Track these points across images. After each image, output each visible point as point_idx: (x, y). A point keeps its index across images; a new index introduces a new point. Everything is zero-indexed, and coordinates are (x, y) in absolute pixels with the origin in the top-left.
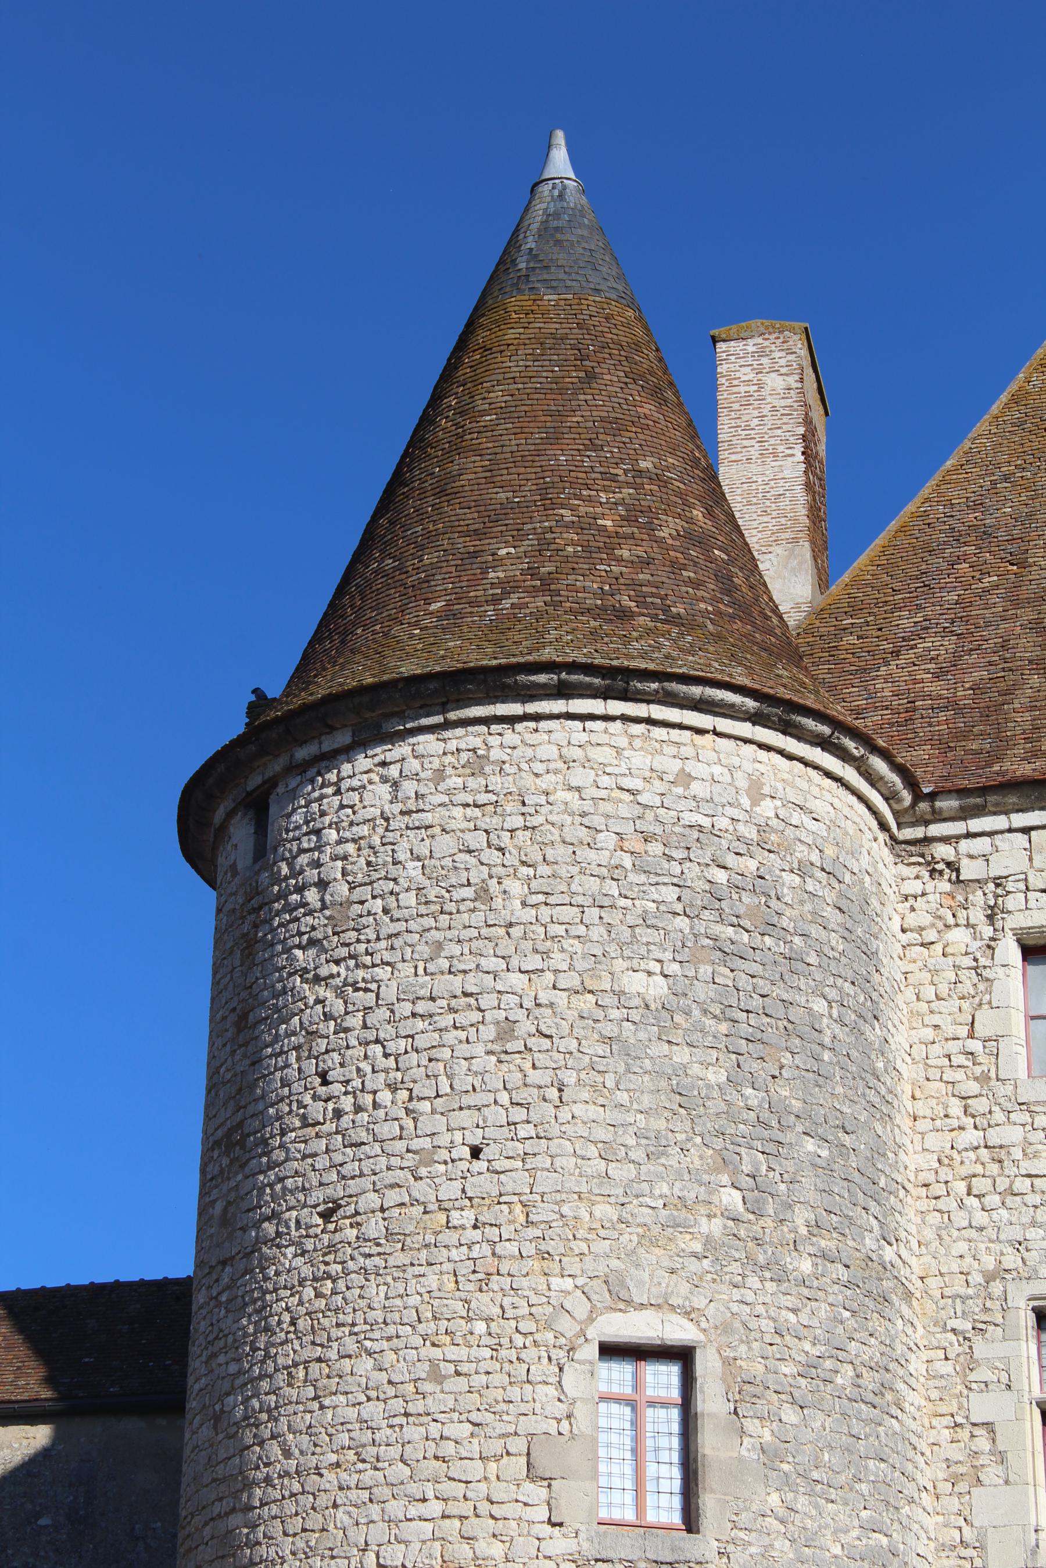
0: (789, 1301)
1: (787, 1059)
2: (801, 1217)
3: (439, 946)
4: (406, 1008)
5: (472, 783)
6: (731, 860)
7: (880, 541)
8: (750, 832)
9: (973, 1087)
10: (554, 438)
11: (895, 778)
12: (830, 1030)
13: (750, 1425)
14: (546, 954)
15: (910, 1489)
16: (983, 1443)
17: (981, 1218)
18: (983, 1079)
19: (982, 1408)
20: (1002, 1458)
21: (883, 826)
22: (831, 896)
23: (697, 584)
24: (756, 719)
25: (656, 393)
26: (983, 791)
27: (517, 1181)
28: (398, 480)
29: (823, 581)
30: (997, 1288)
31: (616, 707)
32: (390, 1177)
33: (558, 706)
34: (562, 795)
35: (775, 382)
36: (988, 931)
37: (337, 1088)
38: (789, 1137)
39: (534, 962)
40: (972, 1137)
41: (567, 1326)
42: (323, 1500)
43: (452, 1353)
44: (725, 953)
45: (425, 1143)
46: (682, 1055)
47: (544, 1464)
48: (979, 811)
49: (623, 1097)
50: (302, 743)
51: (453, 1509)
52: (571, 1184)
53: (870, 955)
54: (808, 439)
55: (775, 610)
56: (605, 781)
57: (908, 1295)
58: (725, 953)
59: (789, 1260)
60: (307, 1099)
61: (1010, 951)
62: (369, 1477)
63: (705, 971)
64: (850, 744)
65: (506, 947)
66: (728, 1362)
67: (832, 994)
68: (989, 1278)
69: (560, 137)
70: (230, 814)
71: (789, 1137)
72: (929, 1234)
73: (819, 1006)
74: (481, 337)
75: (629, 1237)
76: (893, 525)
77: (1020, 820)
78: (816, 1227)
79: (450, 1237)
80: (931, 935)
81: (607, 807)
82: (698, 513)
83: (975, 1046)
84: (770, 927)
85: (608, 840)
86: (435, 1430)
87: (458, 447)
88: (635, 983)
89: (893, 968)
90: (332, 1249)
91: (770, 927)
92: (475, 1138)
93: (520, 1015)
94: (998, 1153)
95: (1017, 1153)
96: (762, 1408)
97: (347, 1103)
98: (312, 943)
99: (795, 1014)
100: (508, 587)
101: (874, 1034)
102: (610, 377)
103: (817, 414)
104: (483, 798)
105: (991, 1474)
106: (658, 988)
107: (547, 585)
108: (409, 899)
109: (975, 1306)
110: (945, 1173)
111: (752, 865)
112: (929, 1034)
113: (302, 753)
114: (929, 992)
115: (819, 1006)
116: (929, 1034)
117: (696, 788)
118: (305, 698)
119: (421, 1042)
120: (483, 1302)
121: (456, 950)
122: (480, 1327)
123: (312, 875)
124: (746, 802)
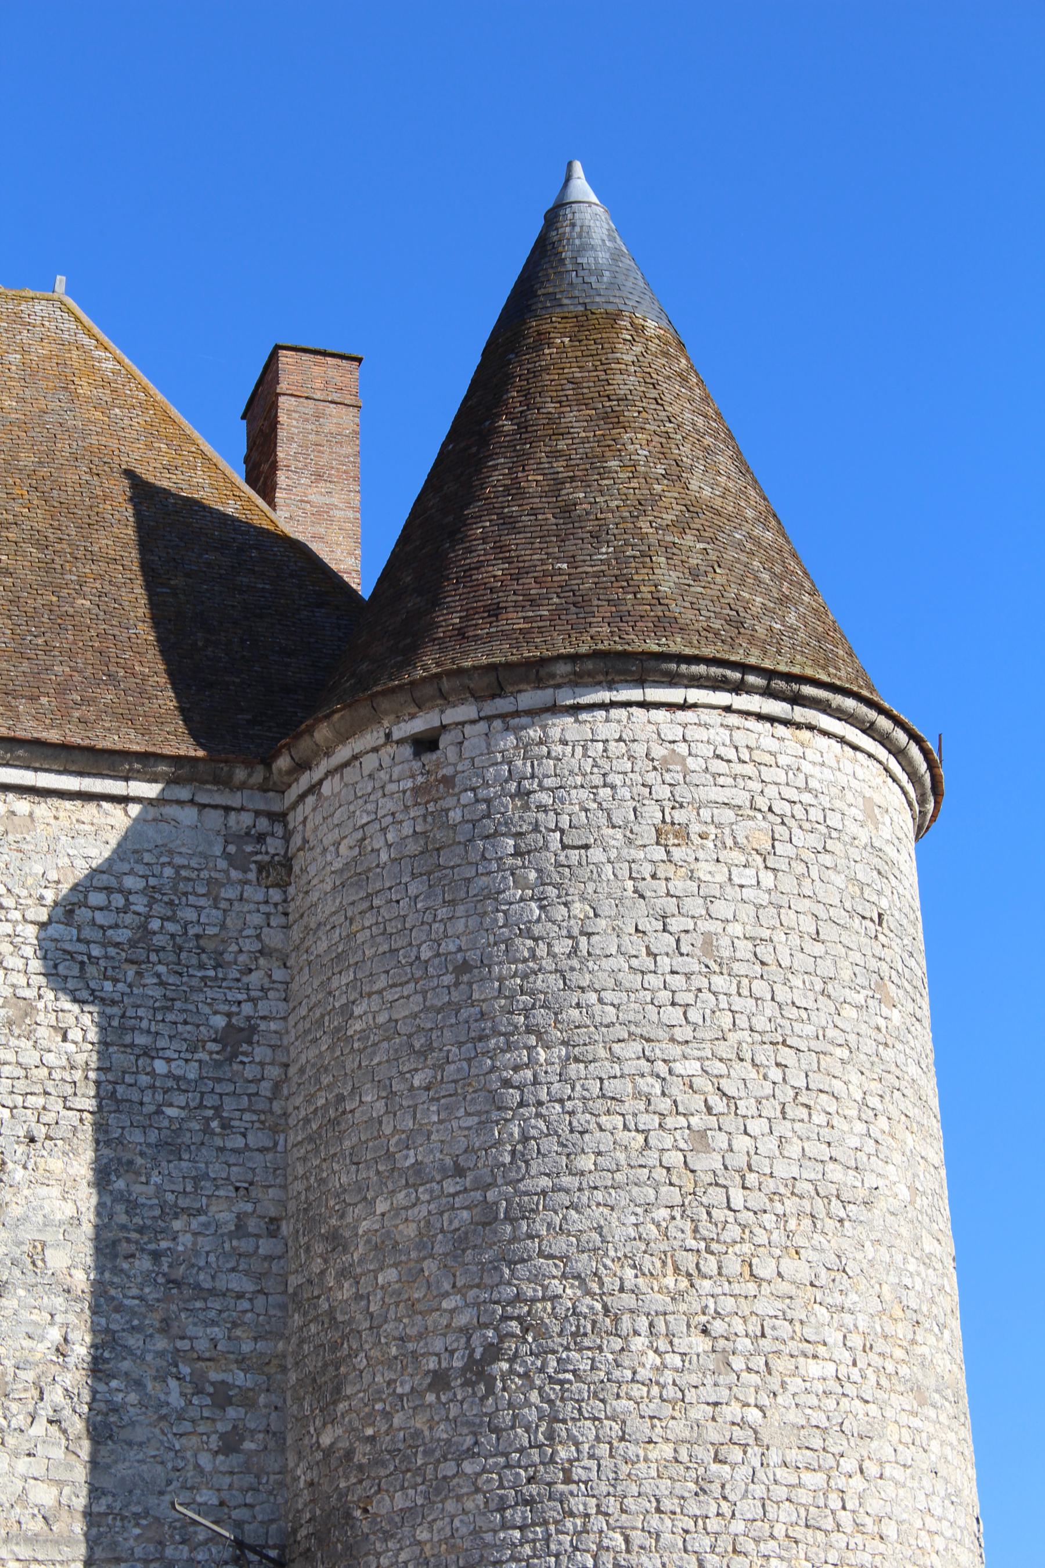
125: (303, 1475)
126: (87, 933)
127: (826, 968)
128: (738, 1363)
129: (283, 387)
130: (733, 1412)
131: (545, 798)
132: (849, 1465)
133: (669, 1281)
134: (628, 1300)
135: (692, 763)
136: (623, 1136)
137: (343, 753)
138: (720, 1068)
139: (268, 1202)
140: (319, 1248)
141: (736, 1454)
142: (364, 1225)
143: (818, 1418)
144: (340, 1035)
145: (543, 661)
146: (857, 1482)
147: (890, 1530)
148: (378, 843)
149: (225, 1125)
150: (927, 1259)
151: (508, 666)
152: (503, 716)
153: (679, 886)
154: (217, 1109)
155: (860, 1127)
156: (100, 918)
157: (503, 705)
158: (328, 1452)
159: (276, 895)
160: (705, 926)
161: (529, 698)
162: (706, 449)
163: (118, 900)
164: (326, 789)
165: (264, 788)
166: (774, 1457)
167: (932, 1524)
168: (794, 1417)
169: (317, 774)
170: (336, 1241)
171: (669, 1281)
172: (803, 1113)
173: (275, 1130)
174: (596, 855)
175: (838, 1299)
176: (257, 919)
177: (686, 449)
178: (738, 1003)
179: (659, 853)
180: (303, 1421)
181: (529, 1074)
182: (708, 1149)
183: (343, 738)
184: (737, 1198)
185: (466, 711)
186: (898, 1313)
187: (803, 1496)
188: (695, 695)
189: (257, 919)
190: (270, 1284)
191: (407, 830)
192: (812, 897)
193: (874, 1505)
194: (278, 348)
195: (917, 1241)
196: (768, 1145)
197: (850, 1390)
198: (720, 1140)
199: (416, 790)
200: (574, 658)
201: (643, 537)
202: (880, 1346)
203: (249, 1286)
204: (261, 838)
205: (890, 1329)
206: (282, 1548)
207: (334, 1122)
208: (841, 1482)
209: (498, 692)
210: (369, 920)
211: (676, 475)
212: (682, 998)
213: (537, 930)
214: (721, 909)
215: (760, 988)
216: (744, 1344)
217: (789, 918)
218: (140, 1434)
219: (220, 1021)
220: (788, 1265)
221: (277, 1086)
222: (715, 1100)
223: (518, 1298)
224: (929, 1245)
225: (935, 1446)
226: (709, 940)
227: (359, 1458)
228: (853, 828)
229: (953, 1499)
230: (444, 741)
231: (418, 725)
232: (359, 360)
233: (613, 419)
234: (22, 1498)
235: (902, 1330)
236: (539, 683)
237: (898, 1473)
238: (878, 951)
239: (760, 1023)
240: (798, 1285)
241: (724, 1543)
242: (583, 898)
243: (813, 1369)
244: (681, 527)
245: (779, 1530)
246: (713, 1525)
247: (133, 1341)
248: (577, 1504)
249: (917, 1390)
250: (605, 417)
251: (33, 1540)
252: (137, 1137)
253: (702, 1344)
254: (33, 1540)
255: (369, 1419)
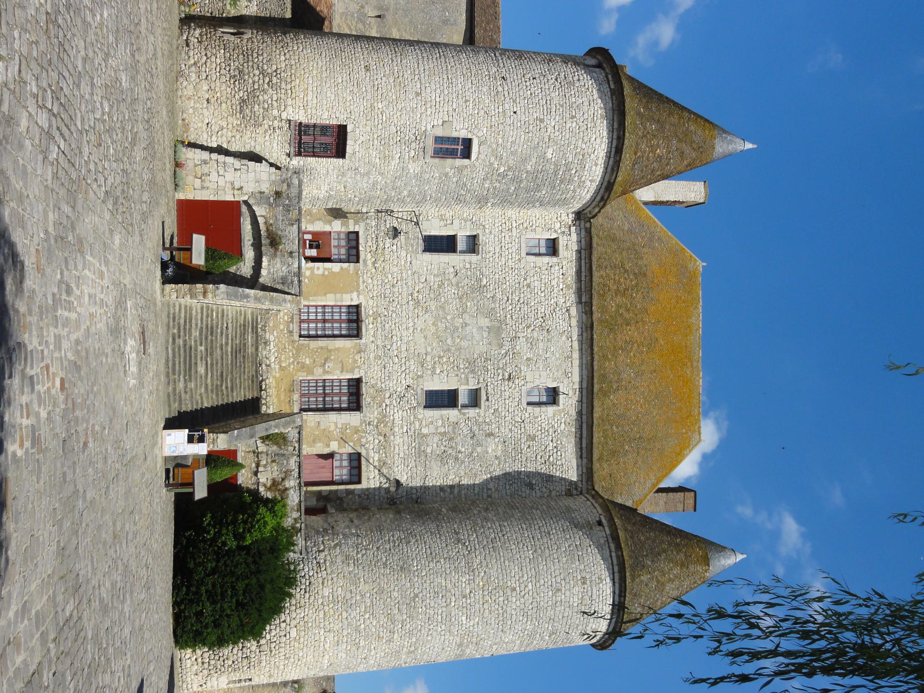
0: (479, 181)
1: (532, 184)
2: (498, 185)
3: (562, 106)
4: (548, 98)
5: (599, 116)
6: (577, 174)
7: (652, 216)
8: (583, 179)
9: (525, 226)
10: (680, 141)
11: (594, 213)
12: (539, 194)
13: (453, 171)
14: (558, 131)
15: (439, 206)
16: (449, 222)
17: (497, 225)
18: (527, 228)
19: (456, 222)
20: (446, 226)
21: (584, 210)
22: (568, 197)
23: (642, 171)
24: (609, 182)
25: (689, 165)
26: (591, 233)
27: (508, 121)
28: (675, 103)
29: (646, 203)
30: (481, 227)
31: (613, 150)
32: (511, 93)
33: (615, 137)
34: (594, 136)
35: (693, 195)
36: (559, 231)
37: (532, 81)
38: (515, 183)
39: (557, 128)
40: (514, 225)
41: (476, 131)
42: (441, 75)
43: (471, 105)
44: (556, 173)
45: (518, 101)
46: (534, 160)
47: (445, 125)
48: (586, 231)
49: (525, 146)
50: (612, 77)
51: (438, 103)
52: (507, 134)
53: (555, 205)
54: (679, 202)
55: (635, 190)
56: (597, 147)
57: (480, 208)
58: (556, 173)
59: (488, 182)
60: (530, 75)
61: (554, 236)
62: (445, 85)
63: (552, 167)
64: (602, 204)
65: (561, 121)
66: (466, 167)
67: (546, 195)
68: (484, 226)
69: (756, 146)
70: (598, 60)
71: (515, 183)
72: (494, 214)
73: (544, 192)
74: (707, 125)
75: (494, 146)
76: (656, 220)
77: (583, 240)
78: (495, 188)
79: (497, 106)
80: (559, 219)
81: (591, 146)
82: (658, 173)
83: (534, 227)
84: (562, 182)
85: (584, 146)
86: (455, 100)
87: (681, 117)
88: (550, 151)
89: (552, 210)
90: (495, 78)
91: (562, 182)
92: (518, 112)
93: (545, 124)
94: (510, 230)
95: (510, 234)
96: (456, 173)
97: (528, 84)
98: (565, 78)
99: (542, 186)
100: (645, 128)
101: (537, 204)
102: (694, 155)
103: (685, 205)
104: (595, 118)
105: (442, 223)
106: (549, 155)
107: (644, 136)
108: (574, 100)
109: (478, 222)
110: (507, 218)
111: (576, 179)
112: (537, 217)
113: (610, 76)
114: (546, 218)
115: (544, 192)
116: (537, 217)
117: (594, 167)
118: (623, 78)
119: (541, 101)
120: (482, 112)
121: (561, 110)
122: (476, 112)
123: (581, 78)
124: (590, 178)
125: (436, 505)
126: (551, 452)
127: (556, 619)
128: (464, 600)
129: (687, 493)
130: (453, 600)
131: (589, 550)
132: (443, 627)
133: (481, 583)
134: (477, 574)
135: (601, 585)
136: (513, 571)
137: (596, 505)
138: (531, 594)
139: (495, 495)
140: (485, 506)
141: (444, 600)
142: (490, 515)
143: (453, 619)
144: (532, 508)
145: (621, 548)
146: (440, 629)
147: (429, 638)
148: (576, 514)
149: (511, 485)
150: (491, 647)
151: (619, 540)
152: (607, 540)
153: (572, 582)
154: (514, 483)
155: (520, 628)
156: (555, 454)
157: (610, 540)
158: (441, 510)
159: (563, 493)
160: (563, 589)
161: (612, 546)
162: (678, 588)
163: (559, 458)
164: (588, 502)
165: (587, 489)
166: (444, 609)
167: (432, 648)
168: (453, 614)
169: (592, 500)
170: (487, 510)
171: (481, 583)
172: (522, 614)
173: (511, 496)
174: (577, 563)
175: (480, 624)
176: (558, 489)
177: (677, 583)
178: (546, 597)
179: (579, 578)
180: (447, 505)
181: (526, 549)
182: (512, 592)
183: (600, 505)
184: (500, 599)
185: (608, 532)
186: (479, 639)
187: (436, 616)
188: (617, 585)
189: (558, 489)
190: (477, 496)
191: (580, 520)
192: (572, 616)
193: (434, 634)
194: (695, 492)
195: (495, 644)
196: (514, 607)
197: (460, 627)
198: (514, 594)
199: (589, 522)
200: (623, 555)
201: (654, 572)
202: (471, 634)
203: (476, 492)
204: (576, 489)
205: (475, 637)
206: (420, 503)
207: (513, 507)
208: (439, 625)
209: (613, 539)
210: (559, 513)
211: (670, 580)
212: (546, 584)
213: (559, 550)
214: (568, 593)
215: (550, 603)
216: (469, 601)
217: (567, 609)
218: (443, 470)
219: (534, 482)
220: (487, 611)
221: (521, 496)
222: (523, 593)
223: (475, 549)
224: (495, 647)
225: (449, 649)
226: (559, 590)
227: (439, 517)
228: (590, 625)
229: (438, 655)
230: (601, 527)
231: (604, 521)
232: (695, 510)
233: (682, 565)
234: (427, 445)
235: (474, 640)
236: (616, 548)
237: (442, 639)
238: (563, 632)
239: (542, 603)
240: (483, 614)
241: (424, 598)
242: (567, 560)
243: (464, 618)
244: (658, 581)
245: (428, 611)
246: (428, 595)
247: (463, 466)
248: (431, 564)
249: (460, 645)
250: (683, 563)
251: (419, 448)
252: (507, 465)
253: (468, 591)
254: (419, 448)
255: (448, 518)
